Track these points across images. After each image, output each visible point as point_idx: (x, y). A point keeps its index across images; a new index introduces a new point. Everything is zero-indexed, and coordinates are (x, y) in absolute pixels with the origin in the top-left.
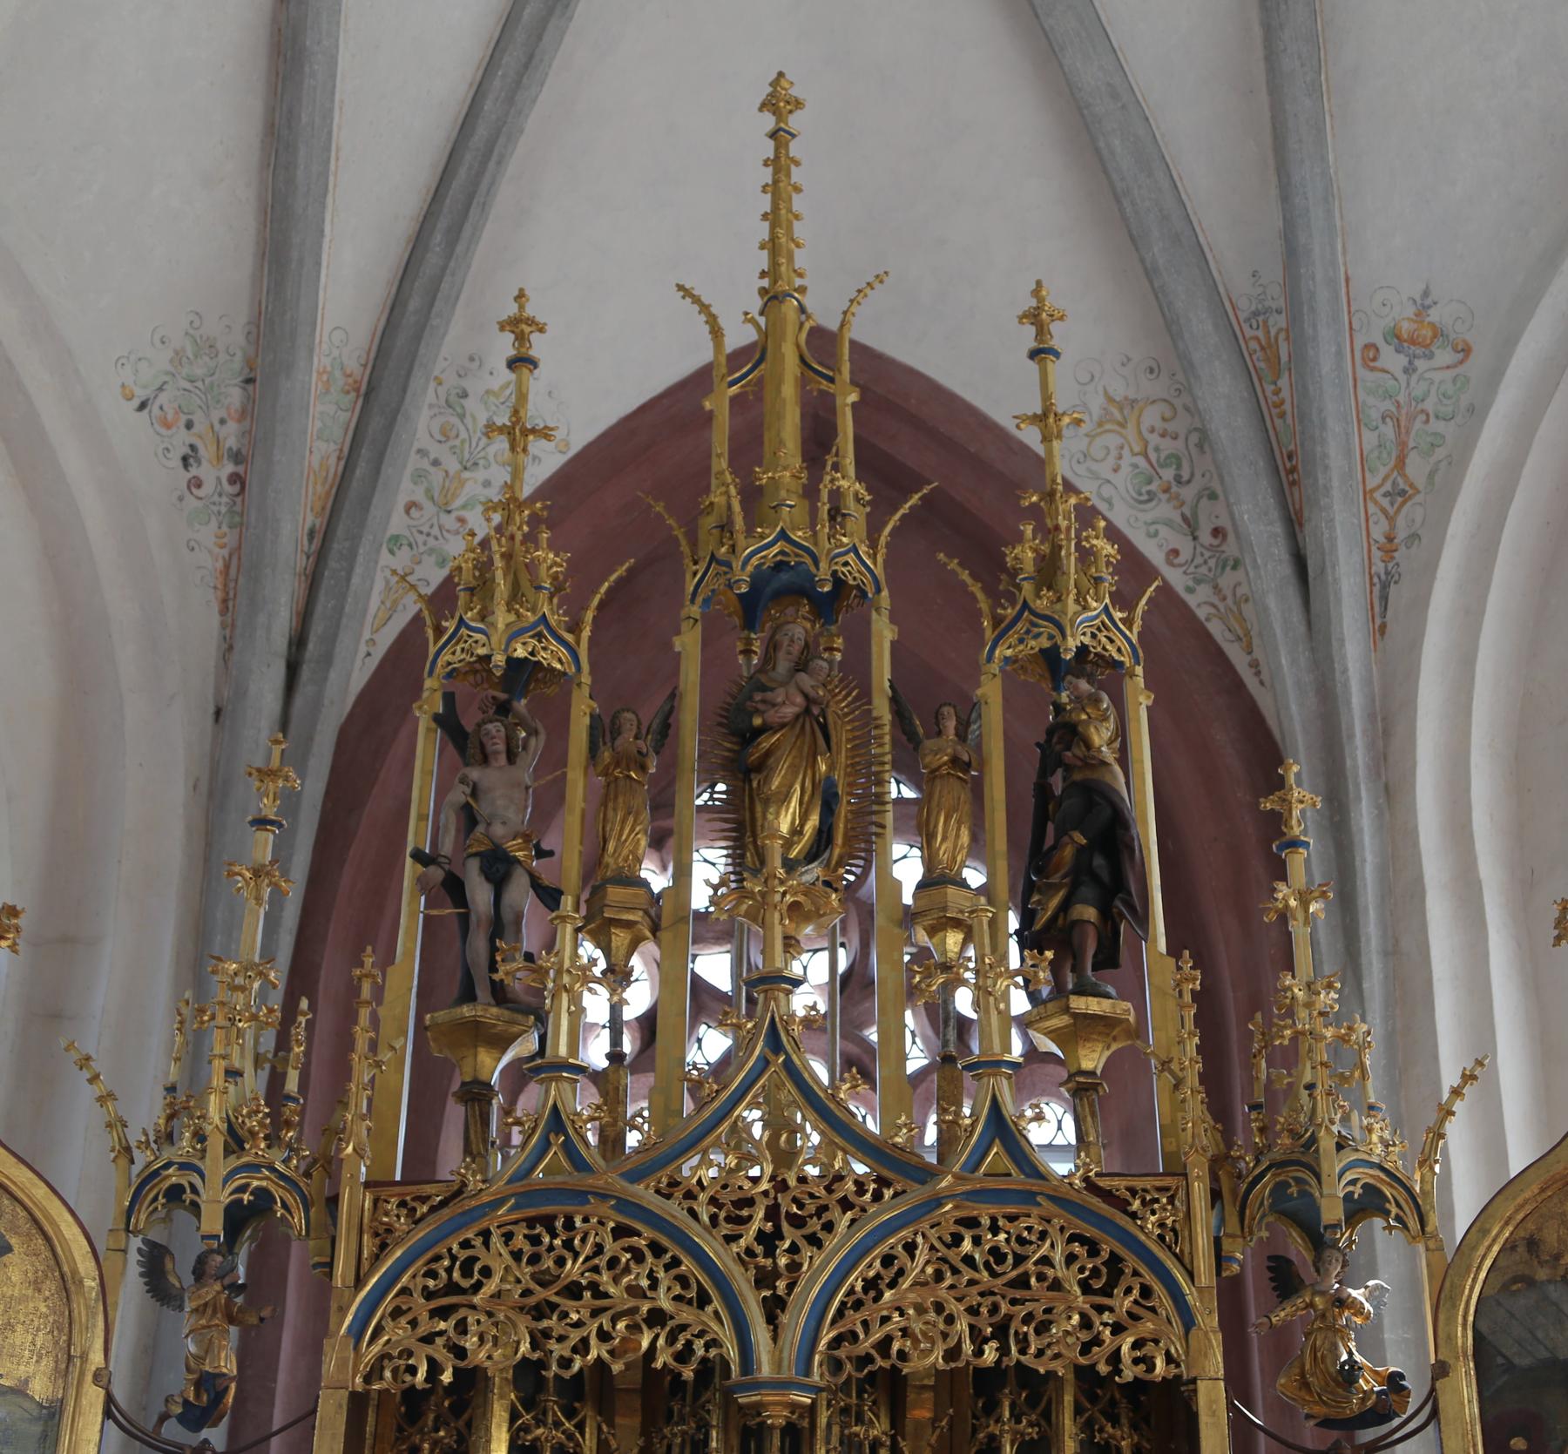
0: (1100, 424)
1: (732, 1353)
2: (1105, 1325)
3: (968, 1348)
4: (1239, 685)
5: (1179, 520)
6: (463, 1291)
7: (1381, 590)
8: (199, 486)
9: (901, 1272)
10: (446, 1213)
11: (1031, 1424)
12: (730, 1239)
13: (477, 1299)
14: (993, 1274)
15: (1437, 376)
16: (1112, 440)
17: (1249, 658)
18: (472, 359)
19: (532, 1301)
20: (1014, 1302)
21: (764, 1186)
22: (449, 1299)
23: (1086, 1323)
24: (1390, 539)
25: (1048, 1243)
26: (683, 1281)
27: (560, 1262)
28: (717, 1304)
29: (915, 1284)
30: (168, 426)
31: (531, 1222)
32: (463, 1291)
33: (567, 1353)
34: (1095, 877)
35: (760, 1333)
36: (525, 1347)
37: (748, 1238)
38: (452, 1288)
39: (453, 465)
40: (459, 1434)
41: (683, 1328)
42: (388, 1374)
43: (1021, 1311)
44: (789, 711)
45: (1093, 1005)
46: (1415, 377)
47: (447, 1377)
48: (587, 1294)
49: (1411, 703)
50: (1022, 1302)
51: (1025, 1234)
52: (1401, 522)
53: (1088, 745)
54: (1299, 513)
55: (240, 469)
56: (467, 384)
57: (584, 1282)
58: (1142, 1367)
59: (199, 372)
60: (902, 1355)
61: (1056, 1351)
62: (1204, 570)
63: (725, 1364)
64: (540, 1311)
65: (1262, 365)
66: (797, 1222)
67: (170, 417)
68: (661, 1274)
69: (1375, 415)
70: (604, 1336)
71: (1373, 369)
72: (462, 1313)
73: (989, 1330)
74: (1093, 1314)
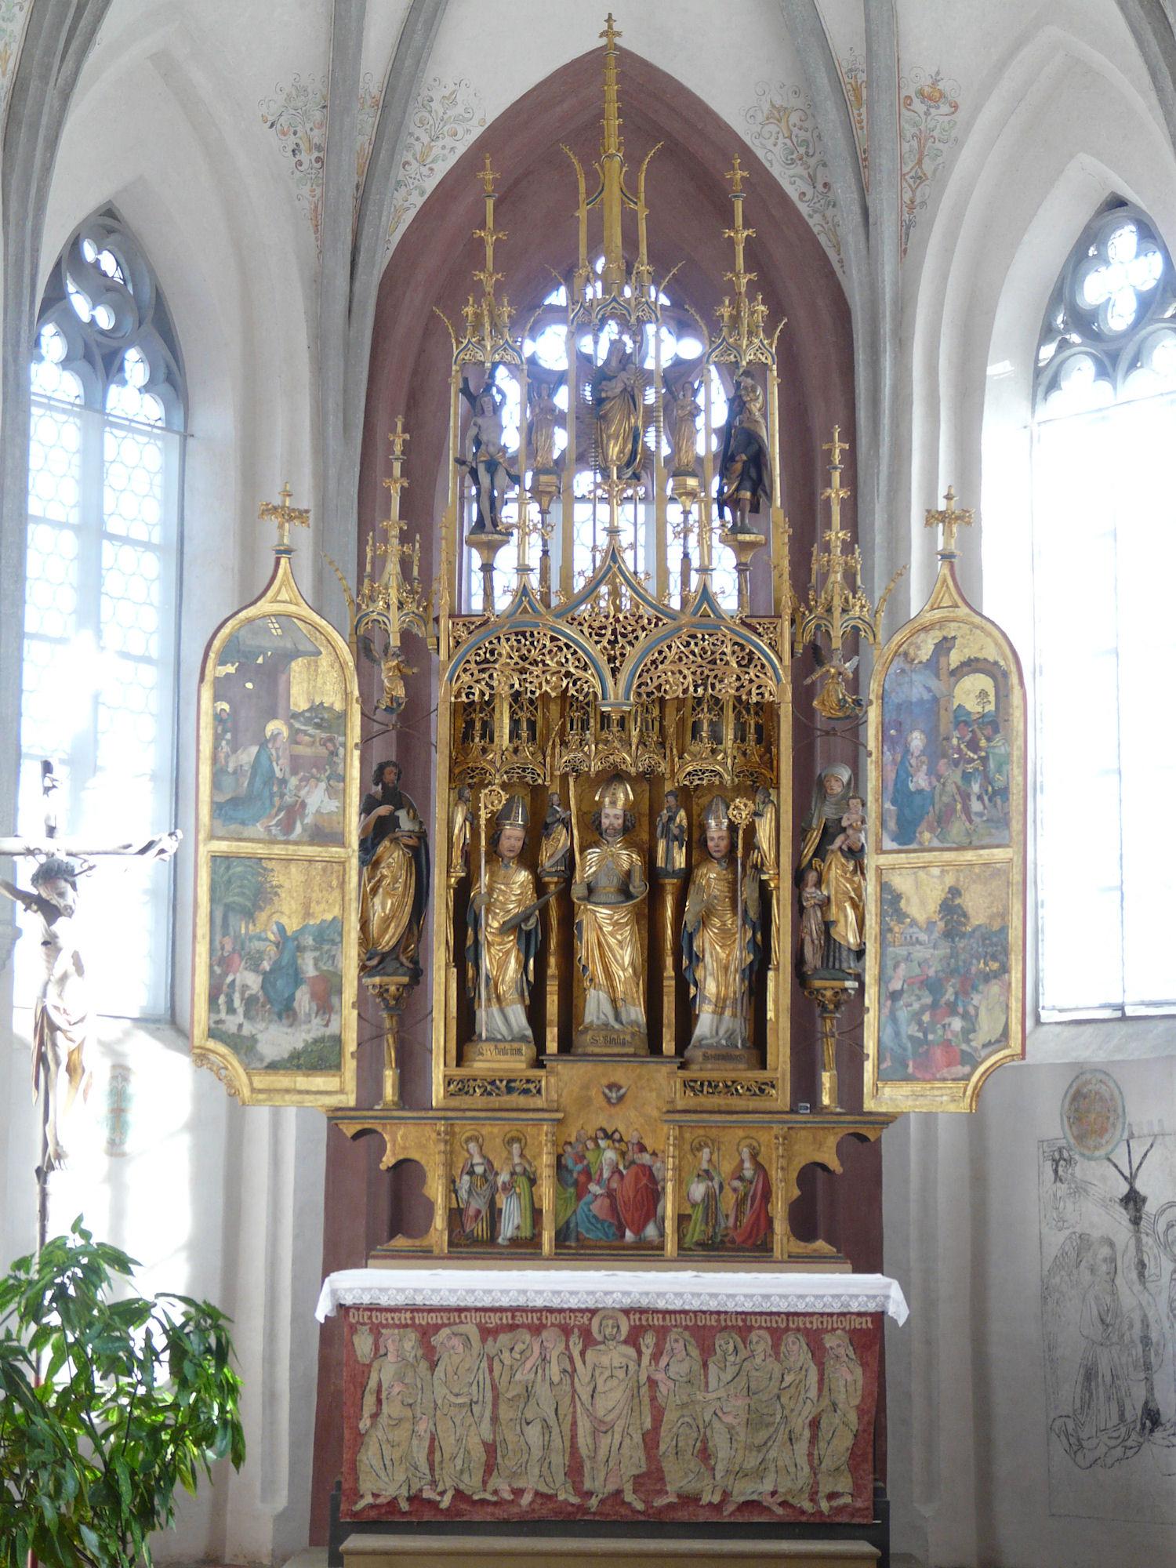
3: (691, 689)
4: (833, 273)
7: (906, 229)
12: (597, 642)
15: (941, 119)
16: (773, 128)
21: (611, 620)
22: (484, 665)
23: (739, 679)
24: (912, 202)
27: (529, 651)
30: (284, 134)
31: (517, 634)
34: (750, 478)
36: (517, 686)
38: (486, 661)
39: (425, 139)
43: (712, 674)
44: (618, 391)
45: (747, 538)
52: (918, 193)
54: (867, 184)
55: (321, 155)
61: (727, 690)
63: (595, 694)
66: (624, 636)
70: (548, 682)
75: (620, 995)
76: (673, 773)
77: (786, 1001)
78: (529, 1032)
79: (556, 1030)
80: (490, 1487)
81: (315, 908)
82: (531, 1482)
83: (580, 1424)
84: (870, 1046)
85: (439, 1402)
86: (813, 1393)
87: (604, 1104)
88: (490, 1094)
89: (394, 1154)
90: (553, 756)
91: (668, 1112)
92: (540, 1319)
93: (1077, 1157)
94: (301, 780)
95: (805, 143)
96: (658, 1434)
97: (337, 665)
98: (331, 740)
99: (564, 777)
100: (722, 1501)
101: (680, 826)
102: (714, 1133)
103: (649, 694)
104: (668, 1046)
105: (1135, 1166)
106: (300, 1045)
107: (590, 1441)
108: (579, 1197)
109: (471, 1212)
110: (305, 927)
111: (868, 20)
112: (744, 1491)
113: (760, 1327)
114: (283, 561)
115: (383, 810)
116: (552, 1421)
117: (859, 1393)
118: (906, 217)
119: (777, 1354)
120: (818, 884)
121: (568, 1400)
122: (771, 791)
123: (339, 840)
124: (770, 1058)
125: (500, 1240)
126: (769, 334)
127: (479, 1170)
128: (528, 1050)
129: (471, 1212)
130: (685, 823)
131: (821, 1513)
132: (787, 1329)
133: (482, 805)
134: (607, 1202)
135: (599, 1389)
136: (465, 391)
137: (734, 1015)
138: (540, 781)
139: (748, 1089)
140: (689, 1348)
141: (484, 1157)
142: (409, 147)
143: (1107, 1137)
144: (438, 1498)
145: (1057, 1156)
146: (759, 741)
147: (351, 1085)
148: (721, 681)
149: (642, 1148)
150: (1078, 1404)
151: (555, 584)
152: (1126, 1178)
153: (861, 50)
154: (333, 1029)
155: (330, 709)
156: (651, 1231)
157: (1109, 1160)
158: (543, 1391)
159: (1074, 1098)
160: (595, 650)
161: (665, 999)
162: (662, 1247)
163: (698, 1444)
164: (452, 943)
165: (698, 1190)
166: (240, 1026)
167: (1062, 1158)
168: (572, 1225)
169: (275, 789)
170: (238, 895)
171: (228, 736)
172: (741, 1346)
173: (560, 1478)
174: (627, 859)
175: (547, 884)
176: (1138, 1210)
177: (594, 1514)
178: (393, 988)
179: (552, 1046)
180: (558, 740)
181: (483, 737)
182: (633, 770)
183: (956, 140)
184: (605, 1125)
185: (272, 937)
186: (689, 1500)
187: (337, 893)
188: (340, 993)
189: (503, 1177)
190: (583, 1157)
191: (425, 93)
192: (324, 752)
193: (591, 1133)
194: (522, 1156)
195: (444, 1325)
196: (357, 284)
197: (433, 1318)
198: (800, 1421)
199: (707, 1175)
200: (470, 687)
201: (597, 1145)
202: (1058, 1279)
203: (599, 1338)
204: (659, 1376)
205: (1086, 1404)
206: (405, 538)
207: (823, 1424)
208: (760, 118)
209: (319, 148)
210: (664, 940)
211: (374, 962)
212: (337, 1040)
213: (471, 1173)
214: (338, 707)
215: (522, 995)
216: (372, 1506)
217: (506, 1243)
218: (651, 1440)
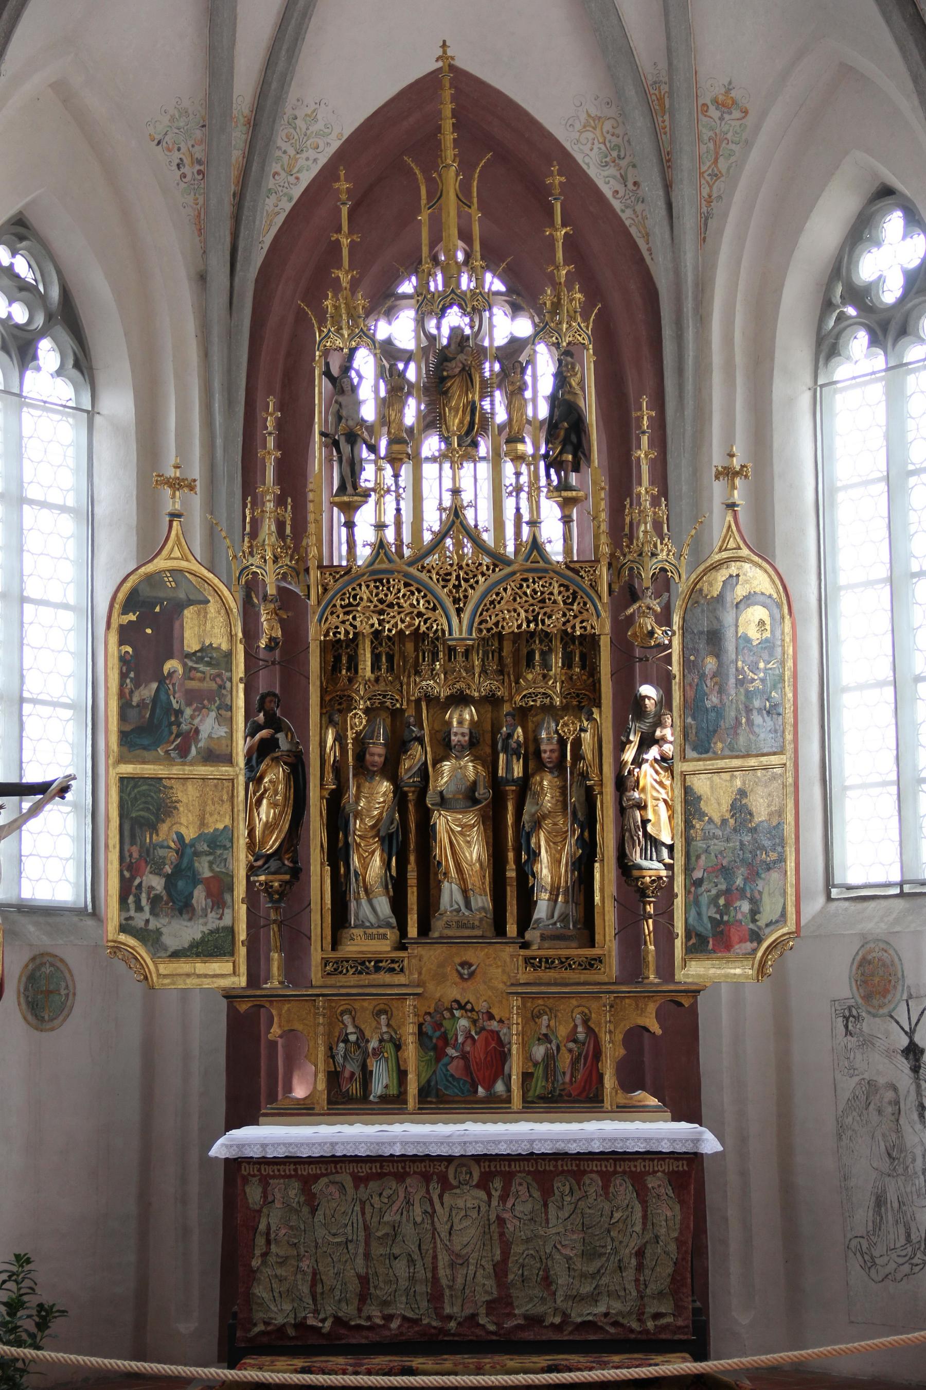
0: (584, 127)
1: (447, 628)
3: (524, 626)
4: (642, 259)
5: (619, 176)
8: (185, 177)
9: (502, 598)
10: (346, 578)
12: (444, 587)
15: (733, 123)
16: (590, 135)
17: (647, 246)
18: (298, 100)
19: (377, 609)
20: (541, 608)
22: (349, 609)
23: (564, 615)
24: (710, 196)
26: (429, 602)
27: (386, 595)
30: (169, 150)
34: (572, 443)
35: (455, 620)
36: (376, 625)
37: (450, 585)
38: (350, 604)
39: (291, 152)
41: (429, 618)
43: (542, 611)
46: (723, 123)
48: (396, 608)
49: (712, 279)
52: (715, 187)
53: (571, 386)
55: (202, 168)
56: (297, 112)
59: (181, 124)
60: (503, 627)
61: (553, 624)
62: (629, 201)
63: (443, 631)
65: (657, 107)
66: (466, 580)
67: (171, 146)
69: (706, 138)
70: (403, 621)
71: (706, 116)
72: (354, 613)
74: (567, 611)
76: (511, 698)
77: (612, 889)
78: (393, 921)
80: (364, 1314)
81: (210, 820)
82: (400, 1308)
83: (440, 1257)
84: (679, 927)
85: (320, 1241)
86: (638, 1228)
87: (458, 980)
88: (360, 973)
89: (280, 1026)
91: (512, 985)
92: (404, 1168)
93: (864, 1014)
94: (194, 711)
95: (617, 147)
96: (506, 1264)
97: (223, 612)
98: (219, 675)
99: (418, 702)
100: (562, 1322)
101: (518, 742)
102: (550, 1003)
103: (489, 630)
104: (512, 929)
105: (914, 1022)
106: (198, 936)
107: (448, 1272)
108: (438, 1059)
109: (347, 1074)
110: (200, 835)
111: (668, 38)
112: (580, 1314)
113: (592, 1171)
114: (175, 523)
115: (264, 733)
116: (416, 1256)
117: (677, 1226)
118: (704, 209)
119: (607, 1194)
121: (429, 1235)
122: (594, 710)
123: (228, 760)
125: (371, 1098)
126: (586, 319)
127: (353, 1038)
128: (392, 935)
129: (347, 1074)
130: (521, 739)
131: (647, 1331)
132: (615, 1172)
134: (461, 1062)
135: (455, 1228)
136: (328, 373)
137: (566, 902)
138: (398, 705)
139: (580, 965)
140: (532, 1190)
141: (356, 1027)
142: (279, 159)
143: (889, 997)
144: (320, 1325)
145: (847, 1014)
146: (583, 667)
147: (243, 969)
148: (550, 617)
149: (491, 1017)
150: (870, 1228)
151: (407, 537)
152: (906, 1033)
153: (663, 65)
154: (227, 921)
155: (218, 649)
156: (499, 1087)
157: (892, 1017)
158: (408, 1230)
159: (860, 965)
160: (443, 593)
161: (508, 888)
162: (508, 1100)
163: (541, 1273)
164: (325, 845)
165: (539, 1052)
166: (147, 921)
167: (851, 1015)
168: (433, 1083)
169: (173, 719)
170: (142, 810)
171: (132, 675)
172: (576, 1187)
173: (424, 1304)
176: (917, 1060)
177: (454, 1335)
178: (276, 884)
179: (413, 931)
180: (413, 672)
181: (348, 670)
183: (747, 142)
184: (459, 997)
185: (172, 845)
186: (534, 1321)
187: (227, 806)
188: (231, 890)
189: (373, 1044)
190: (441, 1025)
191: (288, 111)
192: (214, 686)
193: (447, 1005)
194: (388, 1025)
195: (323, 1175)
196: (237, 279)
197: (312, 1170)
198: (627, 1251)
199: (546, 1038)
201: (453, 1015)
202: (850, 1119)
203: (454, 1183)
204: (506, 1215)
205: (878, 1226)
206: (280, 501)
207: (648, 1252)
208: (578, 126)
209: (199, 162)
211: (259, 863)
212: (231, 931)
213: (346, 1041)
214: (225, 647)
215: (386, 887)
216: (263, 1333)
217: (376, 1100)
218: (500, 1270)
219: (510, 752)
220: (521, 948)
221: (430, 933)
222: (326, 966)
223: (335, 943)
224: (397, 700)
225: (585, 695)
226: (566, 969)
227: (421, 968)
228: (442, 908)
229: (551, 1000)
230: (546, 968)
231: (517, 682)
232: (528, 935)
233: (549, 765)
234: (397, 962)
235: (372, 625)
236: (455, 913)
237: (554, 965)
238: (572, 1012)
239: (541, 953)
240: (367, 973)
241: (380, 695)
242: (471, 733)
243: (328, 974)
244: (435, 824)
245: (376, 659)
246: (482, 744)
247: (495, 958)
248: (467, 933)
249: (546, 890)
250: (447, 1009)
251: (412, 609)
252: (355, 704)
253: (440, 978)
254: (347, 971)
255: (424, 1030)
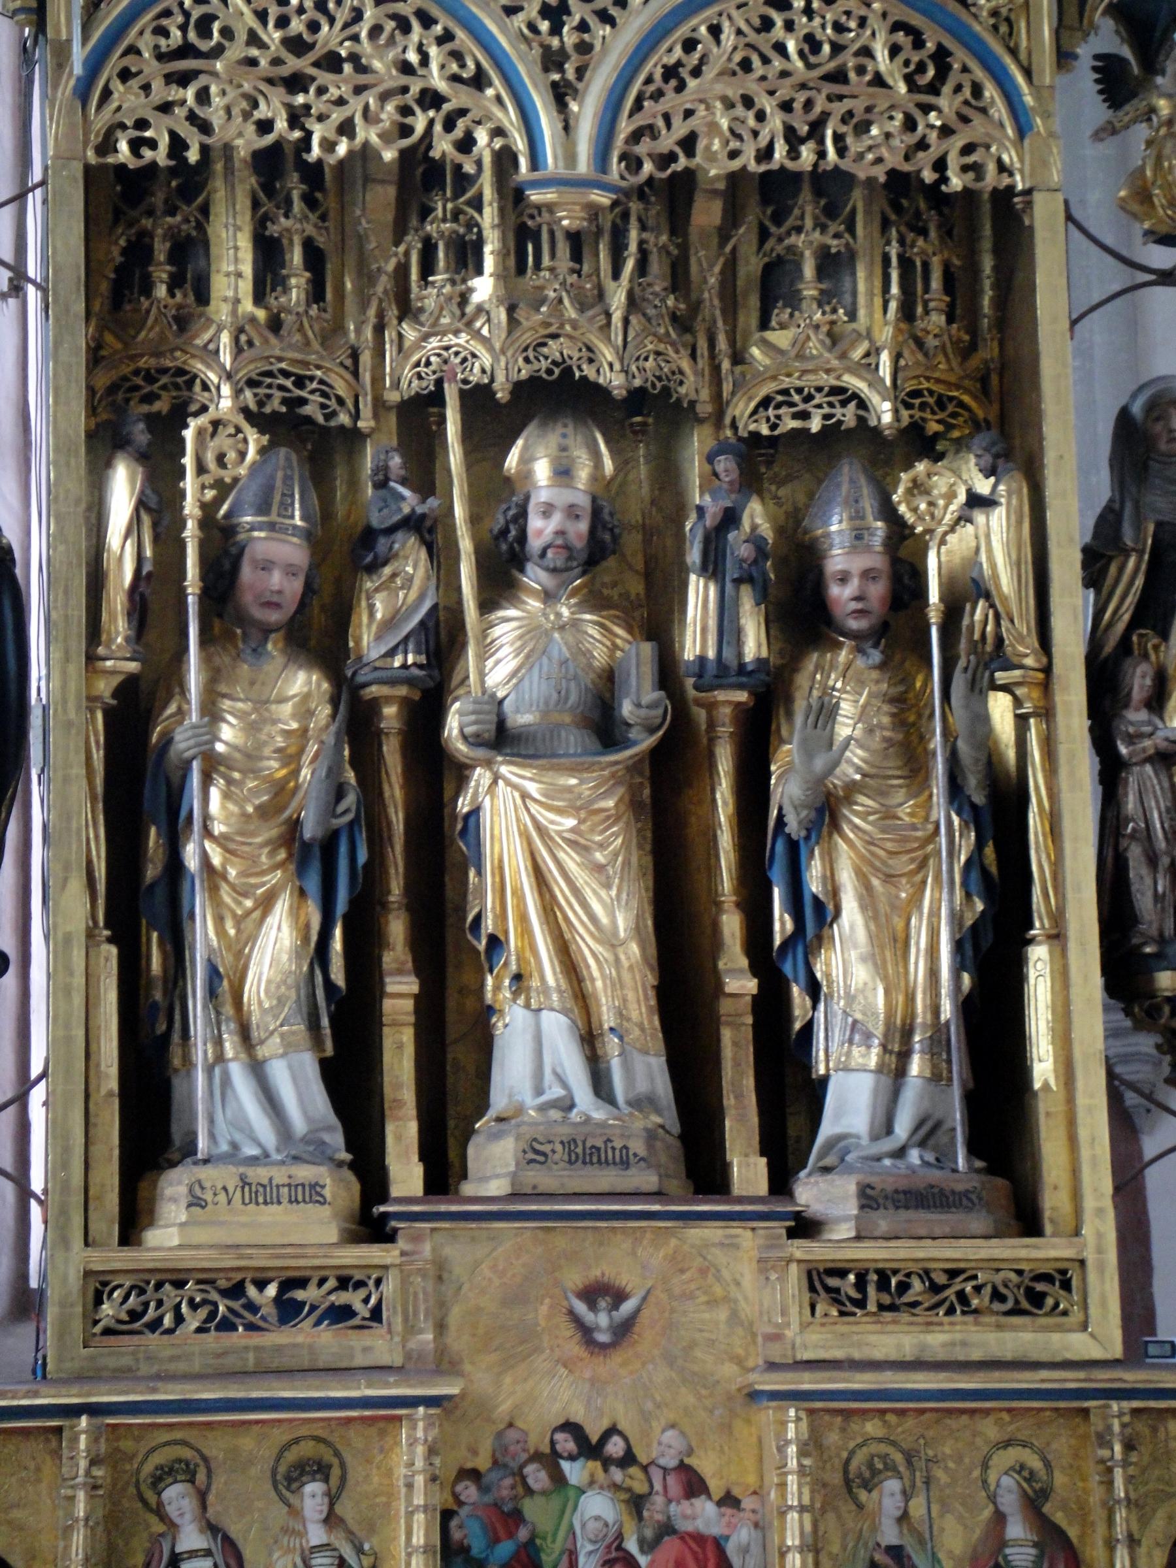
2: (932, 127)
6: (198, 54)
9: (703, 60)
11: (837, 236)
13: (219, 66)
14: (809, 66)
19: (285, 71)
20: (830, 99)
22: (183, 65)
23: (910, 124)
25: (868, 32)
27: (314, 27)
28: (497, 87)
29: (721, 74)
32: (198, 54)
33: (332, 135)
36: (281, 125)
40: (197, 221)
41: (463, 112)
42: (123, 146)
47: (193, 156)
48: (347, 68)
50: (840, 98)
51: (844, 18)
57: (343, 53)
58: (971, 175)
64: (296, 83)
68: (433, 51)
72: (202, 80)
73: (806, 128)
75: (607, 1018)
78: (336, 1139)
79: (413, 1128)
87: (574, 1348)
88: (227, 1326)
90: (380, 353)
91: (772, 1366)
103: (668, 159)
104: (748, 1171)
120: (1157, 702)
124: (1054, 1200)
128: (341, 1190)
130: (766, 530)
133: (188, 461)
137: (937, 1077)
138: (344, 419)
139: (997, 1296)
141: (213, 1529)
148: (863, 128)
149: (694, 1486)
161: (727, 1035)
174: (600, 639)
175: (374, 706)
179: (406, 1175)
180: (392, 312)
181: (175, 283)
182: (614, 381)
184: (578, 1414)
190: (517, 1517)
193: (538, 1441)
194: (331, 1520)
200: (142, 124)
201: (559, 1479)
210: (713, 869)
219: (732, 572)
220: (792, 1234)
221: (468, 1189)
222: (98, 1301)
223: (133, 1221)
224: (341, 401)
225: (961, 404)
226: (951, 1311)
227: (442, 1305)
228: (499, 1101)
229: (910, 1422)
230: (882, 1307)
231: (738, 358)
232: (810, 1193)
233: (854, 624)
234: (361, 1284)
235: (265, 126)
236: (555, 1114)
237: (908, 1298)
238: (985, 1466)
239: (872, 1253)
240: (251, 1327)
241: (286, 374)
242: (596, 512)
243: (108, 1332)
244: (476, 811)
245: (269, 253)
246: (624, 563)
247: (703, 1272)
248: (606, 1179)
249: (868, 1036)
250: (537, 1457)
251: (404, 80)
252: (201, 397)
253: (517, 1346)
254: (179, 1319)
255: (456, 1535)
